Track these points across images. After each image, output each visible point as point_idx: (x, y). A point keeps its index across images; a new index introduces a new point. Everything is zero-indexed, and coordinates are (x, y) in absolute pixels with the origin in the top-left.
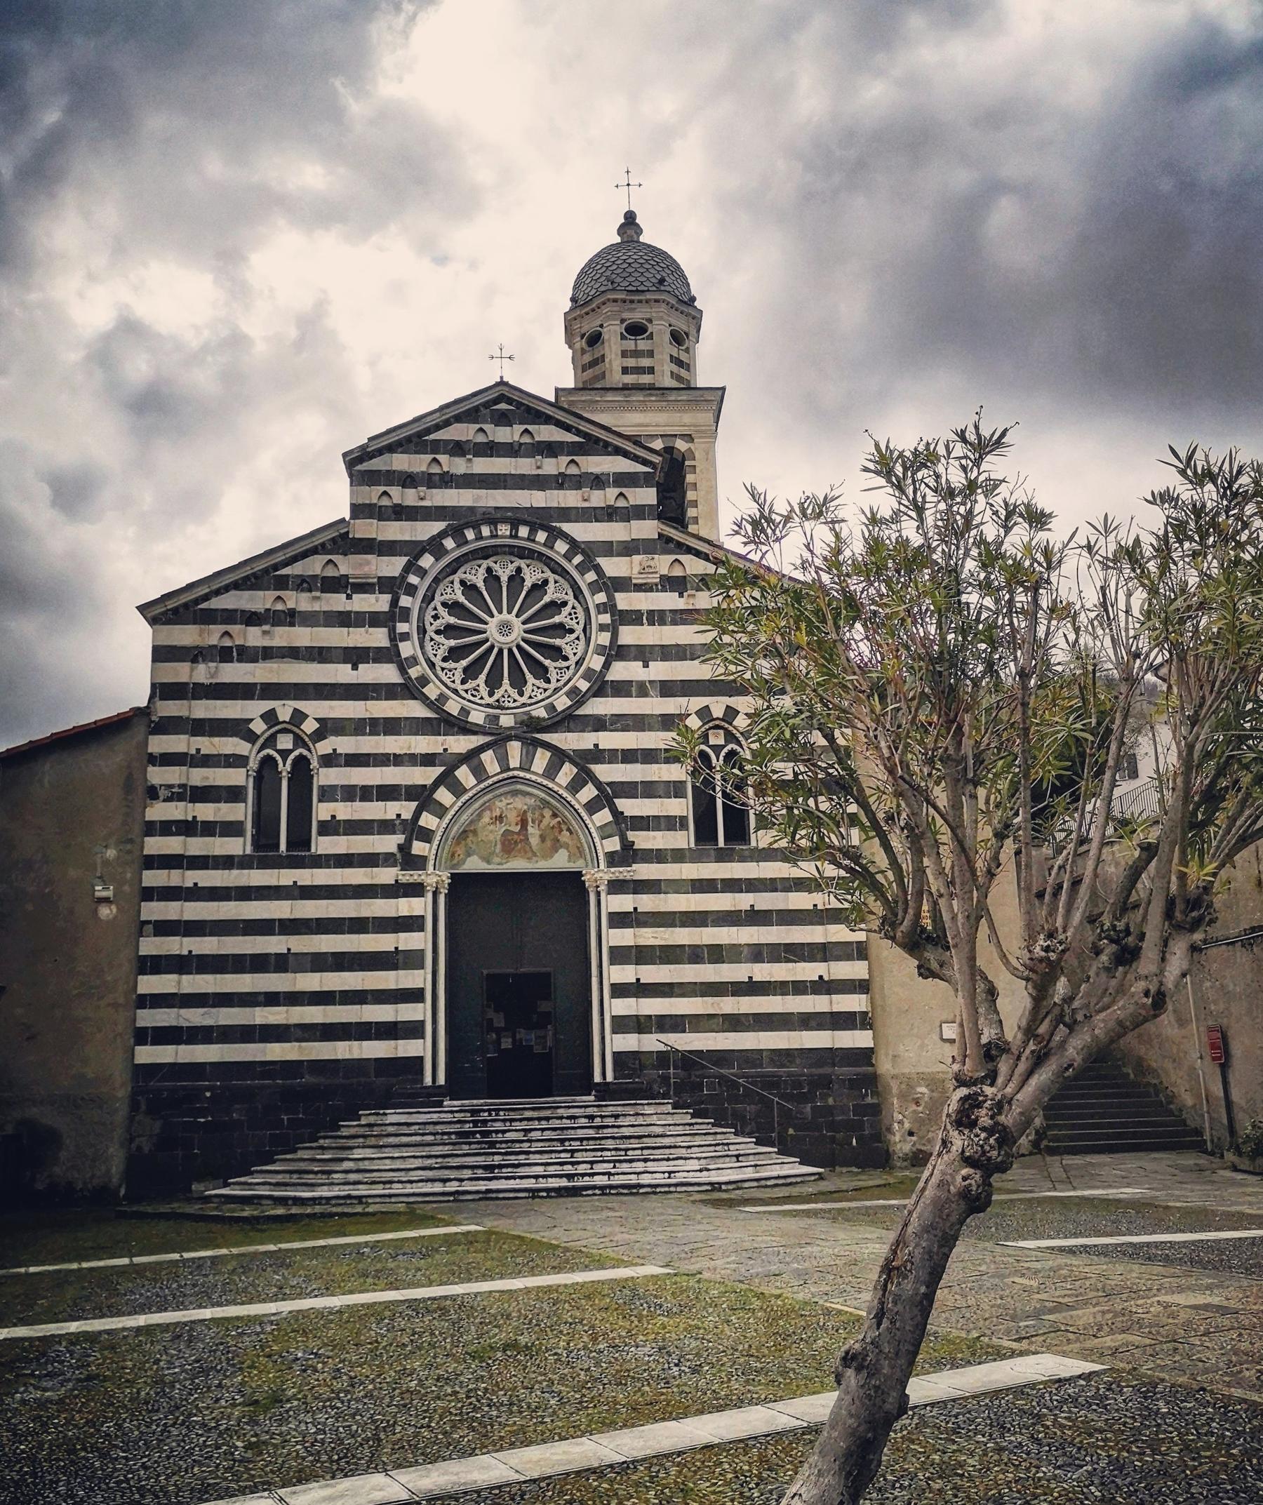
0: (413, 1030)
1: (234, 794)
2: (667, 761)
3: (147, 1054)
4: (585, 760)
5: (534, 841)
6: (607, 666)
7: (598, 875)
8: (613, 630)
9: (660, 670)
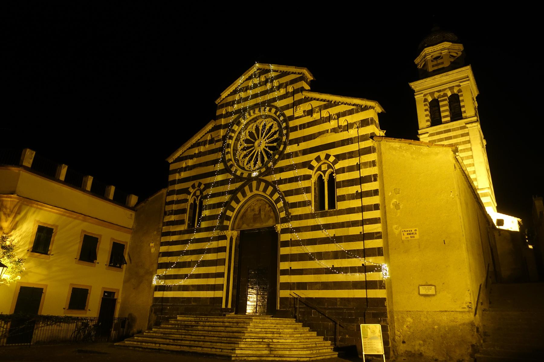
0: (218, 288)
1: (184, 211)
2: (304, 180)
3: (158, 294)
4: (274, 184)
5: (263, 216)
6: (284, 148)
7: (279, 227)
8: (287, 135)
9: (304, 146)
